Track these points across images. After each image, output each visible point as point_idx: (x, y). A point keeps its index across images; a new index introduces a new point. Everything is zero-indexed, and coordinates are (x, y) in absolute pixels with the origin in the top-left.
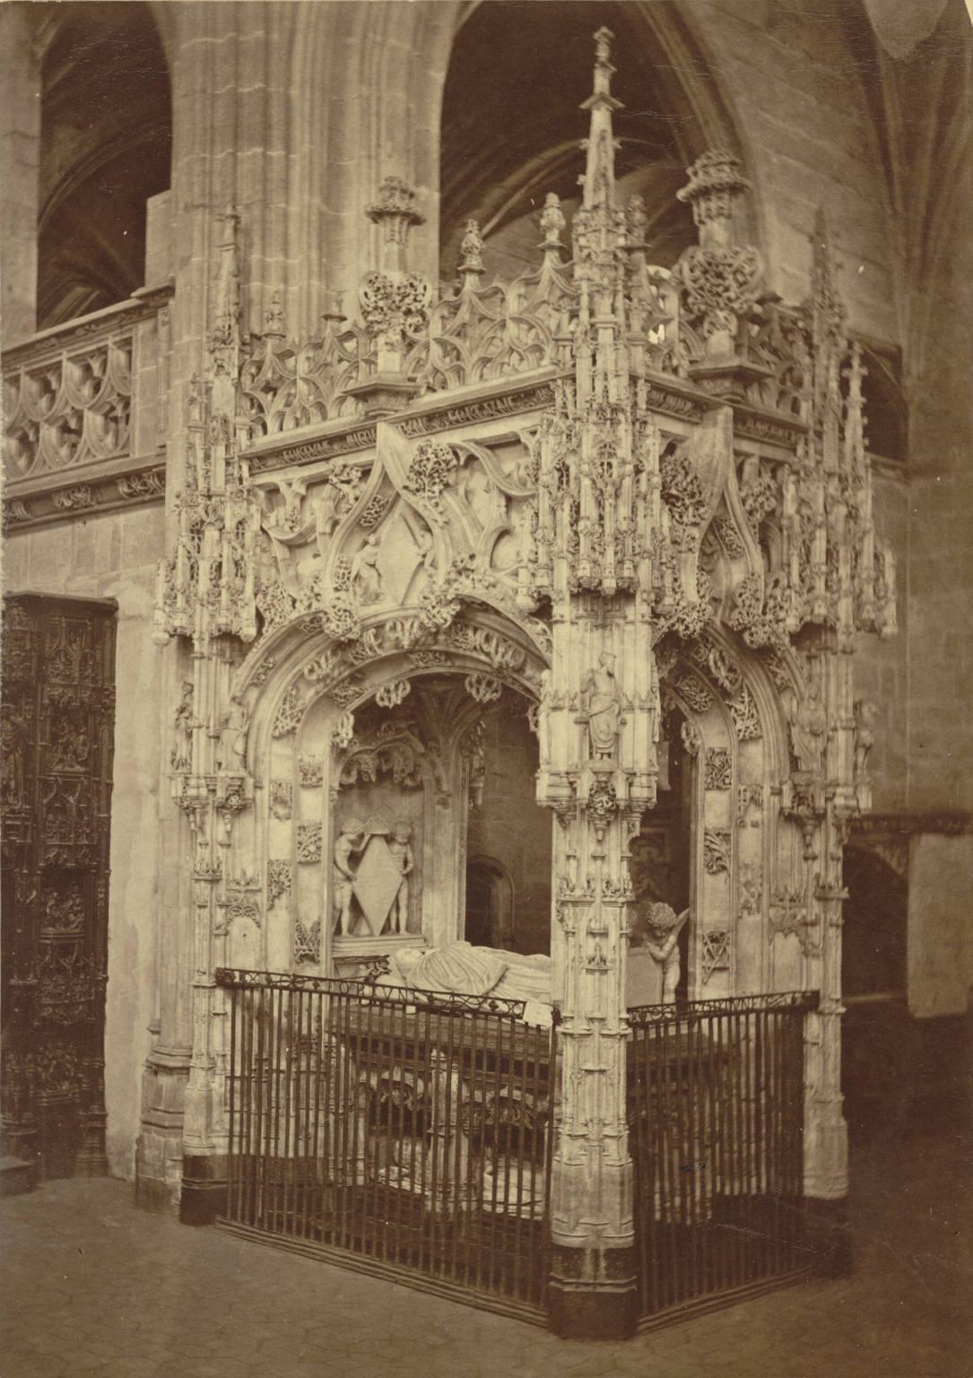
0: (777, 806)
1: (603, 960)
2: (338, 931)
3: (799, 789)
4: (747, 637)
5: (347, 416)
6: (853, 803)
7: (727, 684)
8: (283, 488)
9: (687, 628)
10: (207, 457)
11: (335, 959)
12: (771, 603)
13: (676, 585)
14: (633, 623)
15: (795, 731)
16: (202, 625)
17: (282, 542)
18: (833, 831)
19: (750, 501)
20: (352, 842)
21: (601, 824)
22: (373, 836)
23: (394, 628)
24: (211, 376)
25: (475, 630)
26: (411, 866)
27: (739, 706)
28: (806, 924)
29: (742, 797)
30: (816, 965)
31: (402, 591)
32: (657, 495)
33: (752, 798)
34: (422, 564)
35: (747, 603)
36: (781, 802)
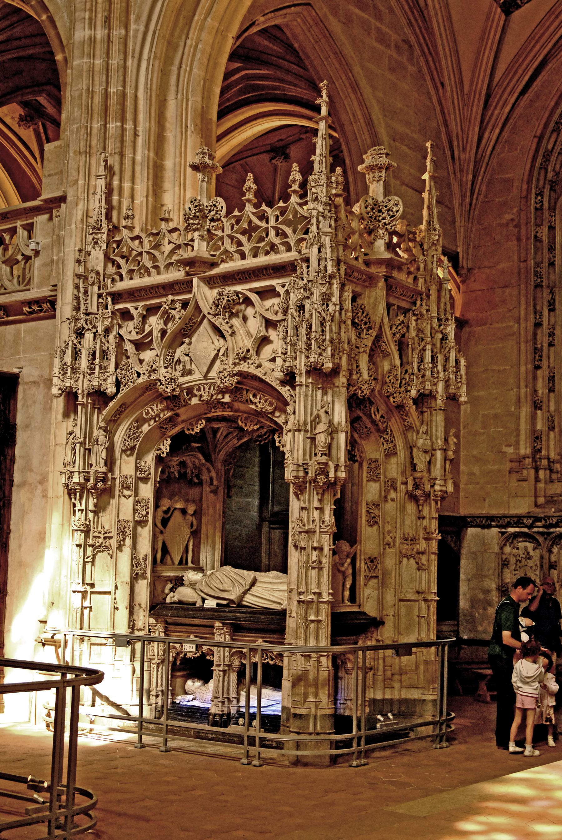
0: (405, 491)
1: (320, 562)
3: (417, 481)
4: (391, 399)
5: (176, 274)
6: (444, 488)
8: (133, 311)
10: (86, 292)
12: (404, 382)
14: (338, 387)
15: (415, 450)
16: (83, 386)
17: (131, 341)
18: (433, 504)
19: (394, 328)
21: (321, 491)
22: (175, 509)
23: (199, 390)
24: (89, 248)
25: (247, 391)
26: (195, 528)
28: (419, 553)
30: (424, 576)
31: (205, 369)
32: (350, 322)
34: (217, 355)
36: (407, 488)
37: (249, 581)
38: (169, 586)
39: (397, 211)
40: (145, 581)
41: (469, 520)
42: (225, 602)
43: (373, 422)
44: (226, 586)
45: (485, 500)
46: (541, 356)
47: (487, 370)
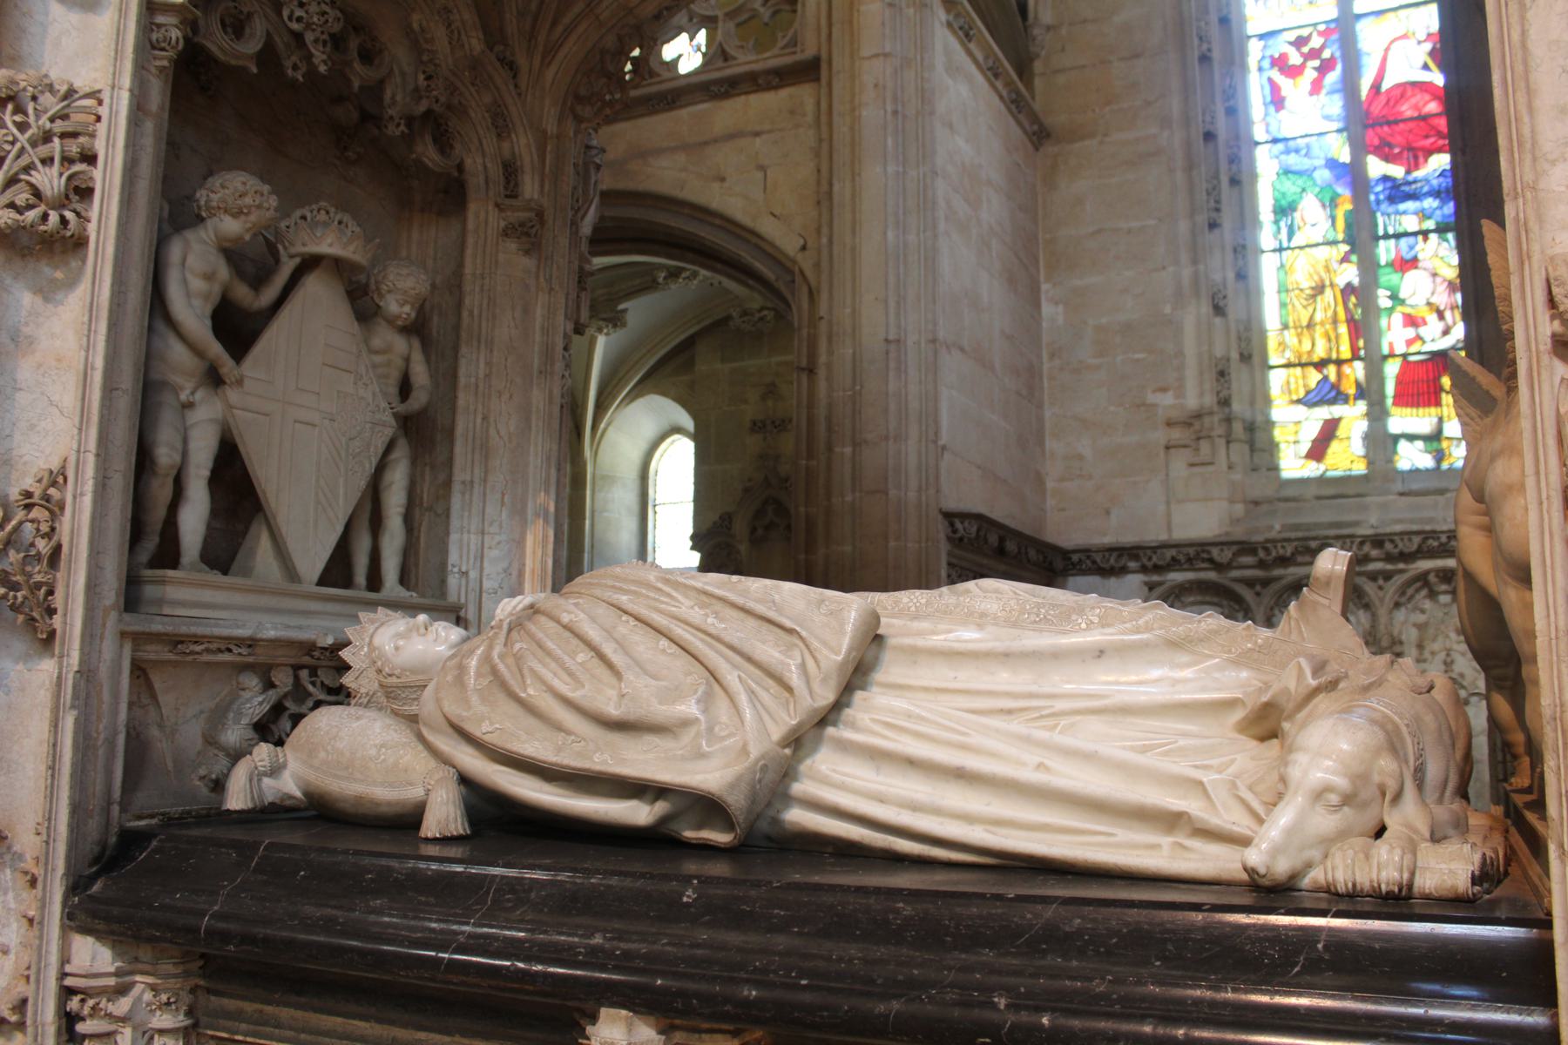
2: (168, 555)
11: (139, 639)
20: (232, 253)
22: (310, 263)
26: (419, 399)
37: (837, 648)
38: (255, 704)
40: (48, 666)
41: (1075, 558)
42: (638, 813)
44: (641, 695)
45: (1108, 512)
46: (1218, 202)
47: (1100, 231)
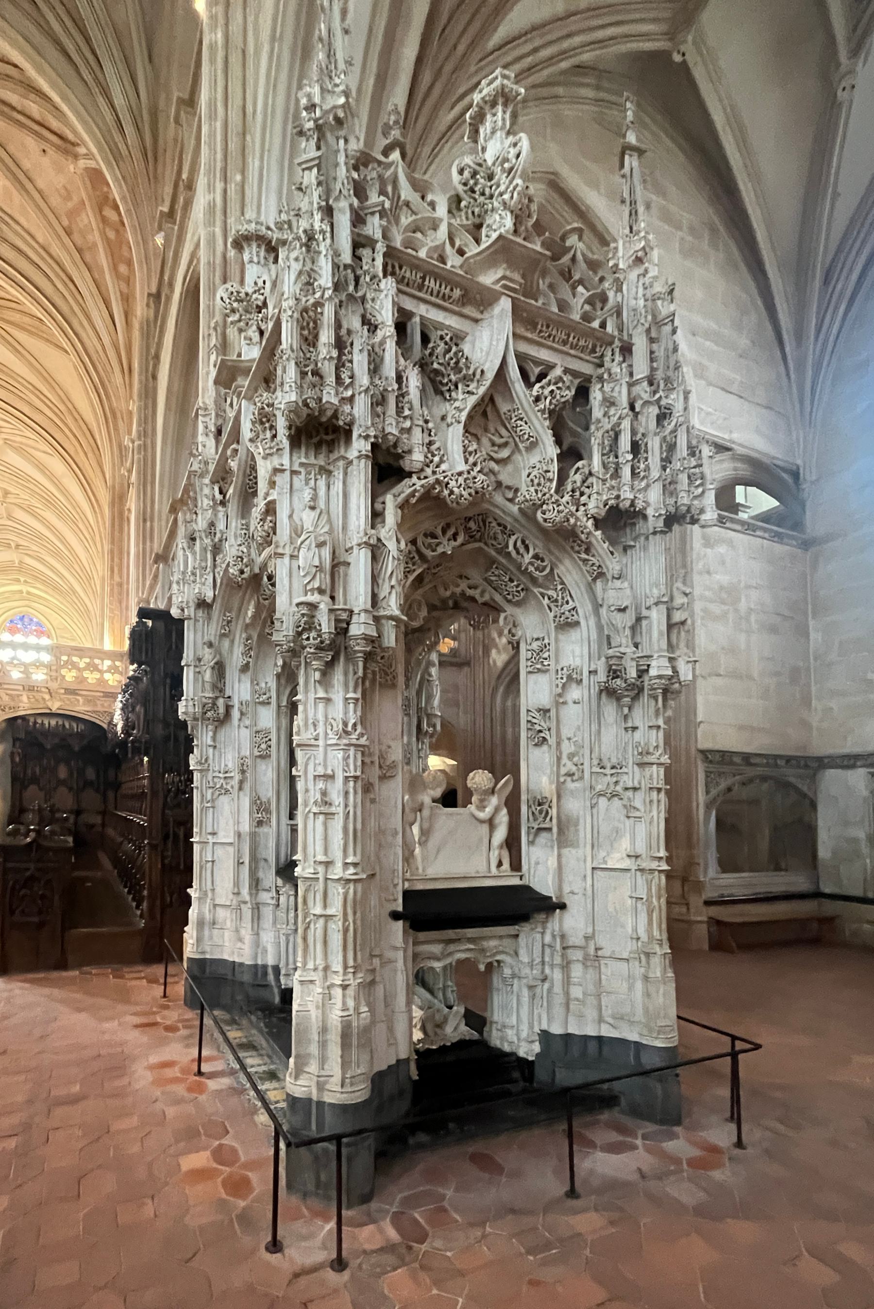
4: (539, 515)
7: (531, 568)
9: (452, 492)
13: (433, 447)
27: (550, 593)
29: (560, 676)
33: (570, 677)
35: (536, 481)
39: (518, 156)
43: (519, 566)
